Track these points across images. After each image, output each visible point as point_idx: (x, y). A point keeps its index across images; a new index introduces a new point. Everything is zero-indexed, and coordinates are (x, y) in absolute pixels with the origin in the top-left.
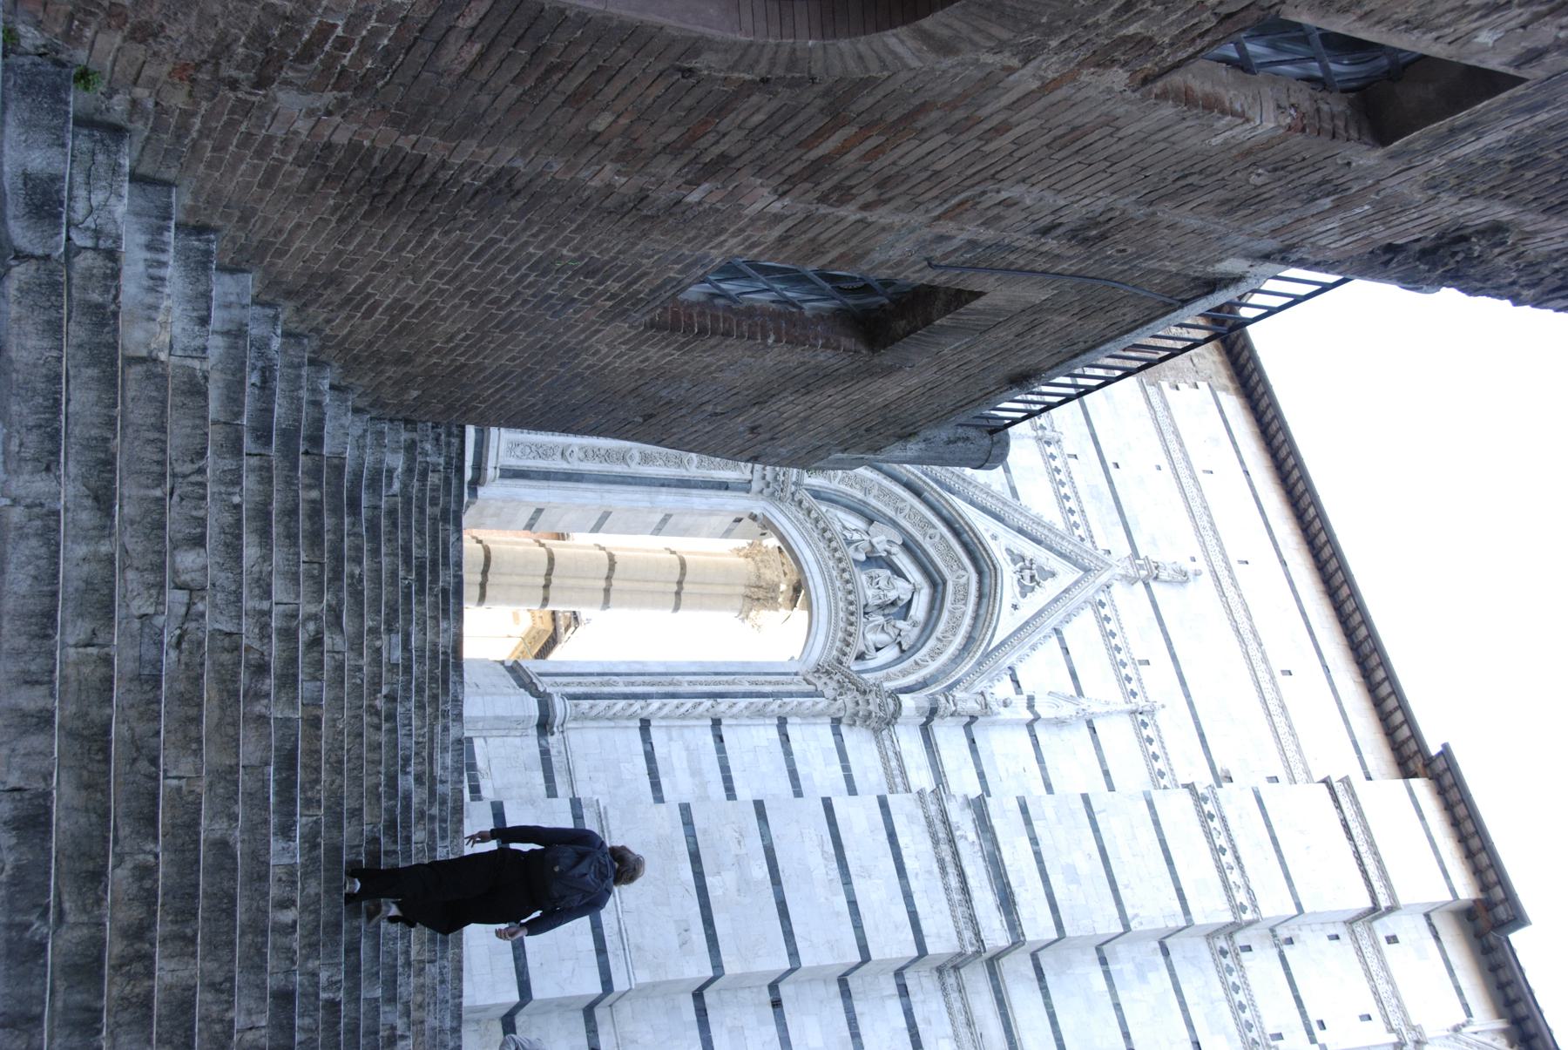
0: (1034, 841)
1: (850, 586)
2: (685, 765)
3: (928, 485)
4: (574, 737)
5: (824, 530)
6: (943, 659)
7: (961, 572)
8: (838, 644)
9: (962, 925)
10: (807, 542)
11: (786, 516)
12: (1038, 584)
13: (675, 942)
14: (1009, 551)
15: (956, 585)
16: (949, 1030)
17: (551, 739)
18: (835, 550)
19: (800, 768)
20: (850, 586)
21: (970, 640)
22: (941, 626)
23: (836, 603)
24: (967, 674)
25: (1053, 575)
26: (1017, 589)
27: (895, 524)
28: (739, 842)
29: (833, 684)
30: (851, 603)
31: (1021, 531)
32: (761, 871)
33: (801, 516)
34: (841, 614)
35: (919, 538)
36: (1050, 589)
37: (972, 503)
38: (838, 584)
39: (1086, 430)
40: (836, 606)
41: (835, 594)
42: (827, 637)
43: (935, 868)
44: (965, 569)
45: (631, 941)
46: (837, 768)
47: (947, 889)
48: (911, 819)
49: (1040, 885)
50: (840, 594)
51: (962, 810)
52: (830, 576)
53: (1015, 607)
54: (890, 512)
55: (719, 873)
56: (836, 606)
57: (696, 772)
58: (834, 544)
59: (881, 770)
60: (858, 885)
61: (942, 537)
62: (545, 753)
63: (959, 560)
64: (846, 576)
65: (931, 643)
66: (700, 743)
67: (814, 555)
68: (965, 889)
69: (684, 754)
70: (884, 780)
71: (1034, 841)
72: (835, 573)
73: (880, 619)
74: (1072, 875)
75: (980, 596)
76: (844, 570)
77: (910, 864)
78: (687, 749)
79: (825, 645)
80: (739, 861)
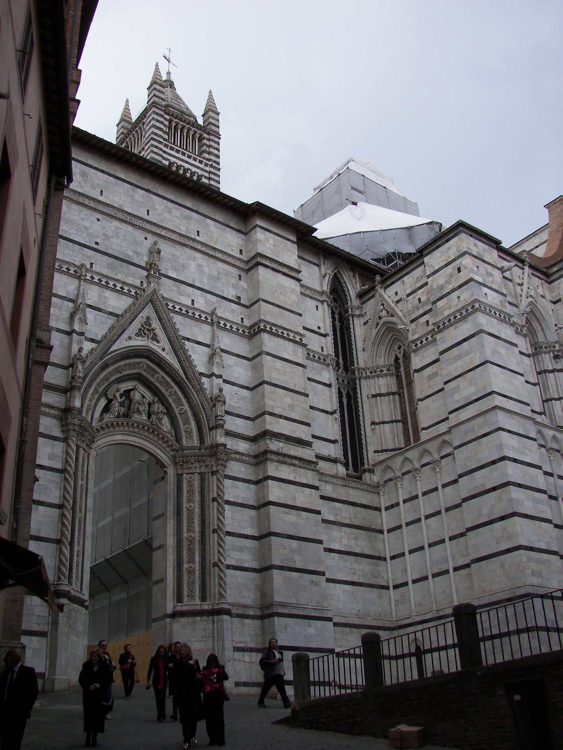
0: (281, 417)
1: (141, 426)
2: (239, 553)
3: (106, 360)
4: (229, 599)
5: (112, 424)
6: (184, 401)
7: (141, 365)
8: (164, 445)
9: (308, 467)
10: (113, 435)
11: (99, 440)
12: (153, 330)
13: (316, 587)
14: (137, 335)
15: (144, 371)
16: (323, 483)
17: (233, 612)
18: (122, 423)
19: (240, 501)
20: (141, 426)
21: (179, 384)
22: (163, 390)
23: (145, 436)
24: (198, 397)
25: (148, 318)
26: (154, 342)
27: (110, 384)
28: (286, 548)
29: (197, 465)
30: (148, 429)
31: (131, 323)
32: (294, 544)
33: (102, 432)
34: (151, 436)
35: (119, 375)
36: (156, 325)
37: (116, 341)
38: (136, 430)
39: (77, 247)
40: (146, 437)
41: (141, 434)
42: (159, 448)
43: (292, 467)
44: (141, 363)
45: (315, 605)
46: (240, 484)
47: (300, 467)
48: (277, 469)
49: (295, 424)
50: (141, 432)
51: (272, 443)
52: (132, 432)
53: (163, 350)
54: (107, 383)
55: (295, 561)
56: (146, 437)
57: (241, 549)
58: (120, 423)
59: (240, 464)
60: (298, 504)
61: (124, 365)
62: (238, 616)
63: (136, 363)
64: (136, 425)
65: (170, 400)
66: (230, 543)
67: (119, 434)
68: (300, 459)
69: (234, 552)
70: (244, 465)
71: (281, 417)
72: (131, 429)
73: (153, 417)
74: (292, 407)
75: (159, 365)
76: (133, 425)
77: (291, 478)
78: (233, 550)
79: (162, 451)
80: (292, 551)
